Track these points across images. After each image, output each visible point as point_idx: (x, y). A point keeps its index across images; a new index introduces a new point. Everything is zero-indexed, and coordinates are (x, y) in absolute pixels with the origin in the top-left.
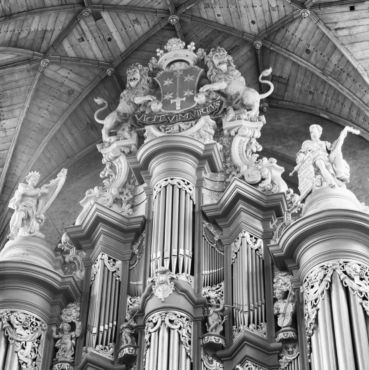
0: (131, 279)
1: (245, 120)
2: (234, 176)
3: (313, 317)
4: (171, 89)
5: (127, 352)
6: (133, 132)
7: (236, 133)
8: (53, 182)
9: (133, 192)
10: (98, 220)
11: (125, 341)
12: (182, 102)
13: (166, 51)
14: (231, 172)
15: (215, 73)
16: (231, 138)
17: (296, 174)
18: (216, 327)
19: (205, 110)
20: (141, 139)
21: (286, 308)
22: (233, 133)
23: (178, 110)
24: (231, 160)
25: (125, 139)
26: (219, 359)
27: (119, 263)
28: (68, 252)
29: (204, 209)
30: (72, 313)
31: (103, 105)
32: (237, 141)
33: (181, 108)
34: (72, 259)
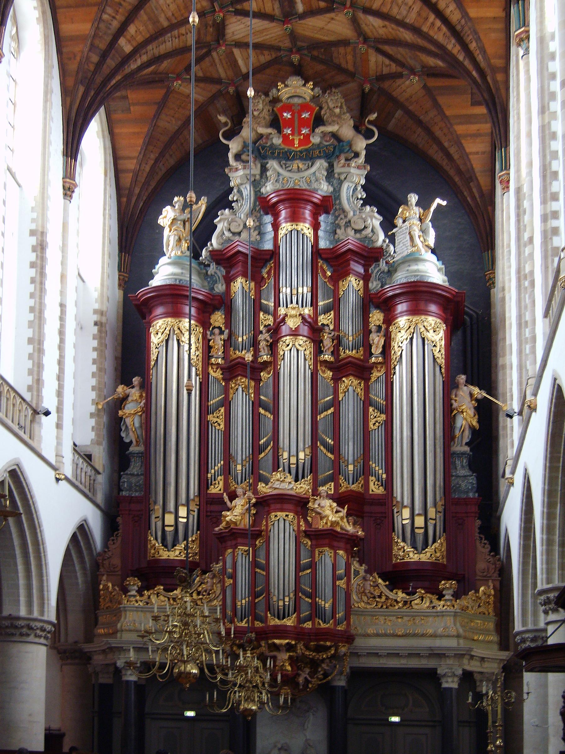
0: (262, 297)
1: (354, 167)
2: (341, 219)
5: (266, 359)
6: (257, 162)
7: (345, 178)
9: (259, 219)
12: (300, 140)
14: (339, 215)
15: (328, 114)
16: (341, 183)
18: (328, 349)
19: (320, 152)
20: (264, 169)
22: (342, 177)
23: (297, 148)
24: (340, 203)
27: (253, 284)
28: (209, 266)
32: (345, 186)
33: (300, 144)
34: (213, 273)
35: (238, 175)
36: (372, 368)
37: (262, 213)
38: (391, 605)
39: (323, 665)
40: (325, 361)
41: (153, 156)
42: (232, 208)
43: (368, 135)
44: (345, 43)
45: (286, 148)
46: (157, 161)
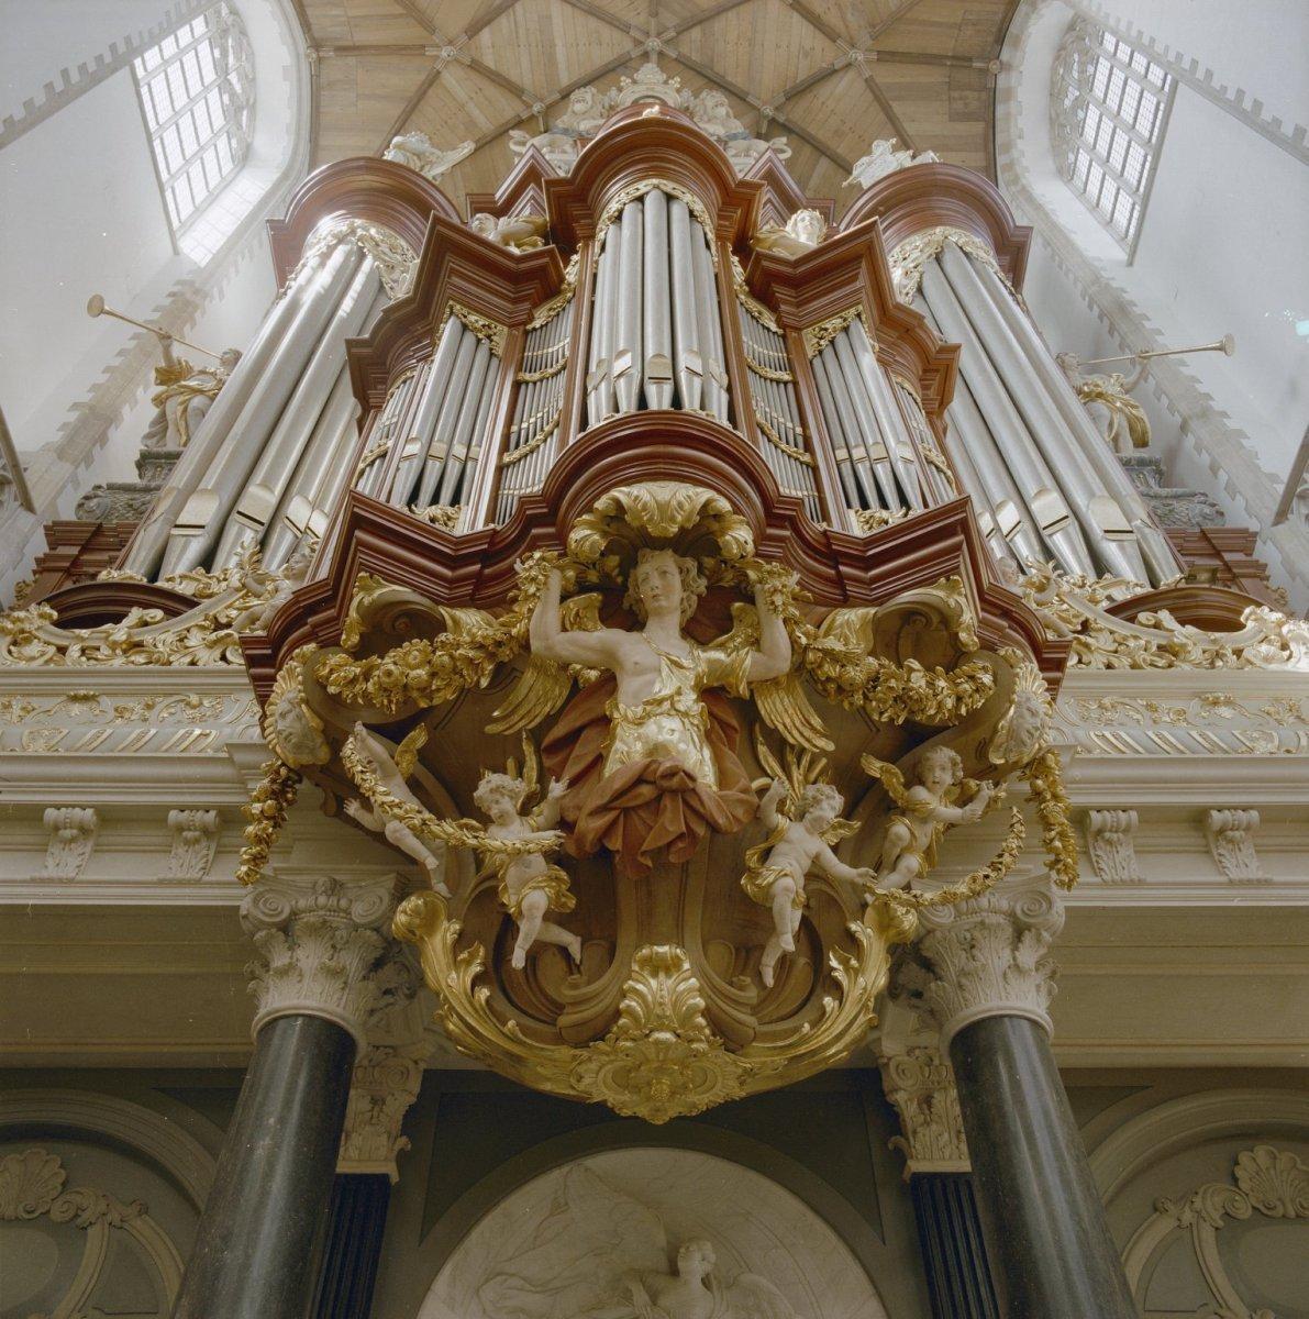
13: (635, 82)
25: (564, 152)
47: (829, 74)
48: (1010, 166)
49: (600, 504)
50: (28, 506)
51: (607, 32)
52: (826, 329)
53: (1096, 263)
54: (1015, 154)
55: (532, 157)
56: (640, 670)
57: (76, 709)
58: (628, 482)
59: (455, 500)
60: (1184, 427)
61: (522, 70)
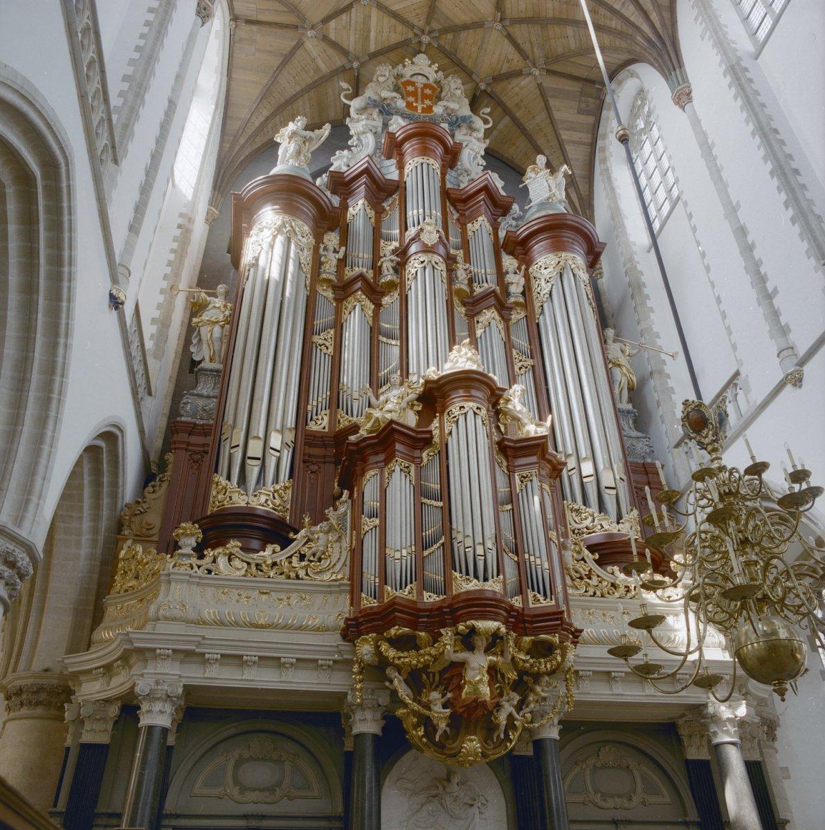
3: (547, 291)
4: (414, 94)
7: (467, 146)
8: (317, 131)
10: (367, 171)
11: (386, 271)
12: (423, 108)
17: (526, 187)
21: (519, 280)
24: (462, 165)
25: (374, 120)
26: (464, 304)
27: (373, 212)
29: (450, 191)
30: (332, 239)
31: (348, 90)
35: (358, 125)
36: (511, 309)
37: (383, 158)
38: (608, 593)
39: (538, 689)
40: (459, 291)
41: (266, 113)
42: (350, 150)
43: (486, 122)
44: (478, 25)
45: (409, 112)
46: (267, 119)
47: (518, 74)
48: (603, 149)
49: (468, 623)
50: (150, 394)
51: (400, 27)
52: (525, 478)
53: (634, 248)
54: (607, 142)
55: (368, 161)
56: (473, 669)
57: (264, 597)
58: (476, 619)
59: (411, 583)
60: (651, 374)
61: (351, 41)
